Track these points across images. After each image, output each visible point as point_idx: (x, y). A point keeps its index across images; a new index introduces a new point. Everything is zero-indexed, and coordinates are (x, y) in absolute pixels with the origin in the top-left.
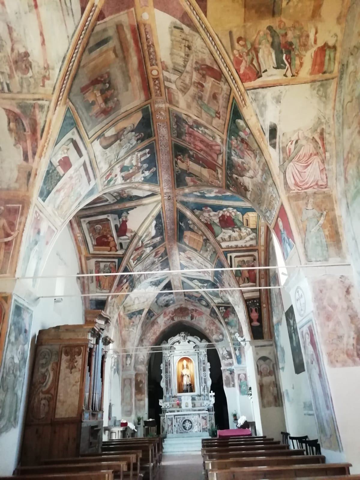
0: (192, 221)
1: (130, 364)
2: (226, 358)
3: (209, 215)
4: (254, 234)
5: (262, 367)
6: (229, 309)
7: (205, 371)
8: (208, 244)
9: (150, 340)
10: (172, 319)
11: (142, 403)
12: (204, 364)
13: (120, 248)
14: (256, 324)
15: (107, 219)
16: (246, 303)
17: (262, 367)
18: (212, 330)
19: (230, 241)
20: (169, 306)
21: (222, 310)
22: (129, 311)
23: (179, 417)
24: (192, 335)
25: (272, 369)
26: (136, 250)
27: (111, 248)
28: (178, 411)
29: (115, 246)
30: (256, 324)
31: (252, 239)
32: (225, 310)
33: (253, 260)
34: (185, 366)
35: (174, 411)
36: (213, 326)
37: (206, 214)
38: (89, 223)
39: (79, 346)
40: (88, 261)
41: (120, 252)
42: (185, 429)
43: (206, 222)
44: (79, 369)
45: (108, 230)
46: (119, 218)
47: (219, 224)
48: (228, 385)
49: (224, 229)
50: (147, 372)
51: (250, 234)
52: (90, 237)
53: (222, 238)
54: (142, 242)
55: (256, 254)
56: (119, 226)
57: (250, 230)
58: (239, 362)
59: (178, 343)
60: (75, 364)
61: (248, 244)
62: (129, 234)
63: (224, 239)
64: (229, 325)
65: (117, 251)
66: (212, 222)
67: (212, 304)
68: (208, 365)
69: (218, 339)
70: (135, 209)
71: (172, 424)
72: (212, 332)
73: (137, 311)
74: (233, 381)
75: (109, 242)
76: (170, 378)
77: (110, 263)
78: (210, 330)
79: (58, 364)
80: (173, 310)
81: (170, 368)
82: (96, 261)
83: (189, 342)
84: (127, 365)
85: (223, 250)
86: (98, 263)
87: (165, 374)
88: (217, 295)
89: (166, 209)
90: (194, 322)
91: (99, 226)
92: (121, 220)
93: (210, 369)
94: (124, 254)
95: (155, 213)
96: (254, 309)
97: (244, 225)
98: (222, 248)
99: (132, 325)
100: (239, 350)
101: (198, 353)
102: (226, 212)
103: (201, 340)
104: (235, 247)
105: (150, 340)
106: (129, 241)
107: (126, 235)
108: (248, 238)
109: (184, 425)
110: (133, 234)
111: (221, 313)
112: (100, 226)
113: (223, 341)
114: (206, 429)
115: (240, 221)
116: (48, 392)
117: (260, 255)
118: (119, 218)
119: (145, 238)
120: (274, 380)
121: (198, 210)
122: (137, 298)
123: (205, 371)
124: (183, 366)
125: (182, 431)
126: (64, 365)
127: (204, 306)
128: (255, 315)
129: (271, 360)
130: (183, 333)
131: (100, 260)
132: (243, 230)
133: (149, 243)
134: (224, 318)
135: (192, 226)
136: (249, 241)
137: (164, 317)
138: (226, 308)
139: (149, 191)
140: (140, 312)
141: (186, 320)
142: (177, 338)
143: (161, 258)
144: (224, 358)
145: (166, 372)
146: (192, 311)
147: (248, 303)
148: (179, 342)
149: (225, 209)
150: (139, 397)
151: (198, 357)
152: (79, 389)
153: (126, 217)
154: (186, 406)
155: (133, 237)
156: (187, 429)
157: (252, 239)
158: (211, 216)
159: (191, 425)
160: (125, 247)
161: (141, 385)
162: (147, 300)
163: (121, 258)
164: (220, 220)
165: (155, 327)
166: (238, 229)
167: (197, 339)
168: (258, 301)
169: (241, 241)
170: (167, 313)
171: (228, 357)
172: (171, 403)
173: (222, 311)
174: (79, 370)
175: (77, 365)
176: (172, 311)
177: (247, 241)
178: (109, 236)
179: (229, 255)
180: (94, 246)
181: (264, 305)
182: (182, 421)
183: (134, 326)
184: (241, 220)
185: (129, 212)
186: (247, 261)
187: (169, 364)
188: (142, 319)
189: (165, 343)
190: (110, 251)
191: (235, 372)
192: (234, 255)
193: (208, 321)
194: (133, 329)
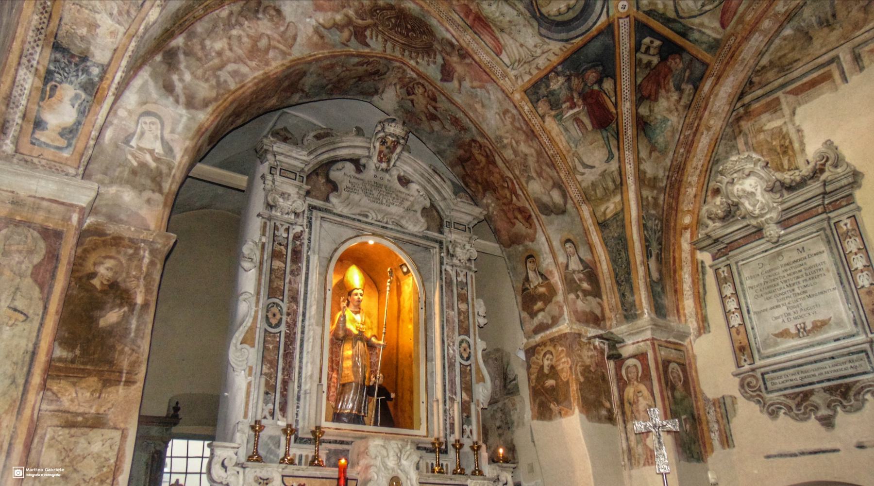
6: (676, 64)
7: (467, 333)
9: (223, 75)
10: (359, 34)
12: (463, 298)
21: (648, 48)
32: (655, 60)
59: (350, 167)
69: (545, 199)
72: (525, 167)
76: (291, 326)
78: (515, 152)
81: (295, 273)
84: (39, 124)
100: (659, 260)
101: (441, 243)
111: (638, 63)
113: (566, 218)
138: (669, 49)
146: (448, 49)
151: (442, 263)
161: (111, 317)
171: (585, 285)
172: (291, 469)
187: (297, 255)
193: (508, 121)
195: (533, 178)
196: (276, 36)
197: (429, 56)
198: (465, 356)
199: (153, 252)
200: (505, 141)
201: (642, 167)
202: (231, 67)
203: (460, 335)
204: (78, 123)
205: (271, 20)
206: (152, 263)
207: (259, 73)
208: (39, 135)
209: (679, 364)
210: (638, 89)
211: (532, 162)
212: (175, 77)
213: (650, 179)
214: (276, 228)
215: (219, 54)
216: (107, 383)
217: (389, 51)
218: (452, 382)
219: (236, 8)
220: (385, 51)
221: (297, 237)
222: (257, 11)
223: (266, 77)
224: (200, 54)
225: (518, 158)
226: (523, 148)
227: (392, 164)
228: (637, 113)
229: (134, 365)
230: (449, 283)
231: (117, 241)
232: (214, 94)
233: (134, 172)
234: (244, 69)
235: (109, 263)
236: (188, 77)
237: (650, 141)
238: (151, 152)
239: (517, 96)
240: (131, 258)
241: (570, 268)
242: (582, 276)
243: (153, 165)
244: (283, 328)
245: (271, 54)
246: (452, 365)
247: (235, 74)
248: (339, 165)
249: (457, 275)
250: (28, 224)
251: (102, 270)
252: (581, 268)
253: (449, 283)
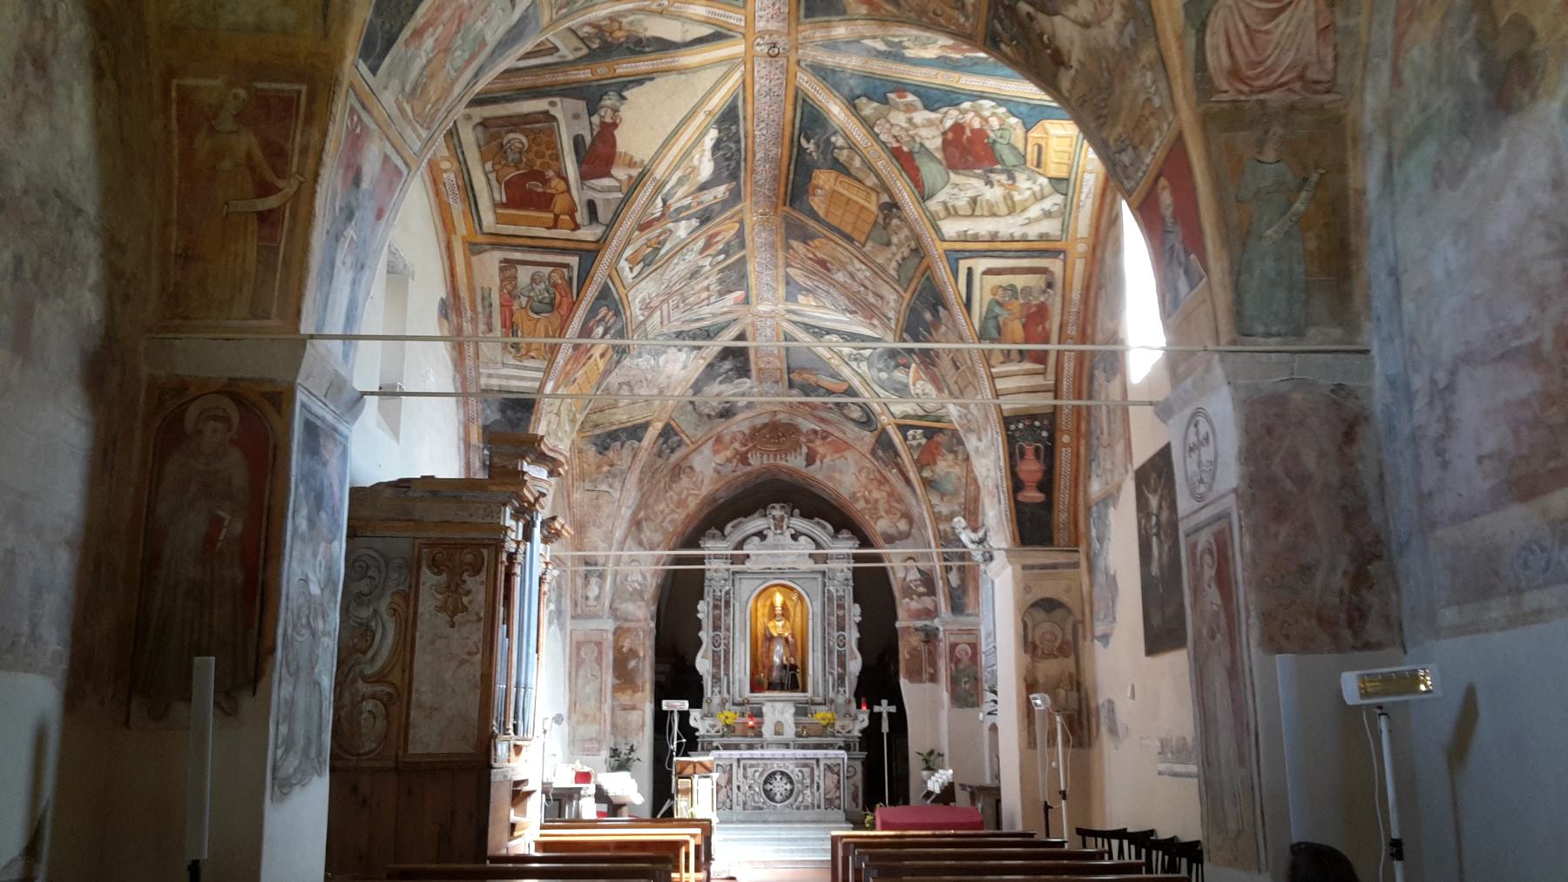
0: (846, 137)
1: (598, 598)
2: (915, 592)
3: (910, 120)
4: (1058, 199)
5: (1038, 632)
6: (939, 438)
7: (843, 630)
8: (895, 222)
9: (665, 524)
11: (634, 716)
12: (841, 607)
13: (586, 222)
14: (1032, 495)
15: (546, 113)
16: (1007, 429)
17: (1038, 632)
18: (877, 501)
19: (972, 215)
20: (735, 414)
21: (914, 438)
22: (596, 426)
23: (754, 762)
24: (807, 515)
25: (1069, 637)
26: (643, 227)
27: (557, 217)
28: (751, 747)
29: (572, 212)
30: (1032, 495)
31: (1048, 214)
32: (924, 441)
33: (1043, 285)
34: (779, 610)
35: (736, 747)
36: (879, 489)
37: (899, 118)
38: (484, 124)
39: (477, 545)
40: (474, 259)
41: (588, 234)
42: (772, 799)
43: (896, 145)
44: (477, 614)
45: (548, 153)
46: (590, 115)
47: (939, 155)
48: (915, 676)
49: (957, 173)
50: (653, 625)
51: (1043, 198)
52: (486, 174)
53: (945, 204)
54: (664, 201)
55: (1055, 266)
56: (588, 140)
57: (1044, 181)
58: (957, 607)
59: (756, 539)
60: (465, 600)
61: (1033, 232)
62: (620, 173)
63: (954, 207)
64: (932, 487)
65: (577, 227)
66: (917, 146)
67: (884, 419)
68: (854, 612)
69: (892, 531)
70: (648, 84)
71: (730, 781)
73: (624, 429)
74: (933, 663)
75: (553, 196)
76: (727, 645)
77: (551, 269)
78: (867, 501)
79: (410, 597)
80: (747, 431)
82: (506, 261)
83: (794, 537)
84: (587, 598)
85: (947, 246)
86: (508, 264)
87: (711, 634)
88: (902, 391)
89: (757, 87)
90: (817, 473)
91: (518, 139)
92: (596, 119)
93: (859, 625)
94: (602, 242)
95: (718, 101)
96: (1029, 449)
97: (1028, 164)
98: (943, 240)
99: (609, 472)
102: (971, 115)
103: (837, 530)
104: (988, 238)
105: (665, 524)
106: (621, 196)
107: (612, 176)
108: (1035, 211)
109: (769, 787)
110: (635, 172)
111: (910, 447)
112: (524, 140)
114: (837, 802)
115: (1014, 148)
116: (380, 678)
117: (1068, 268)
118: (590, 115)
119: (673, 188)
120: (1073, 669)
121: (870, 99)
122: (628, 384)
123: (843, 630)
124: (773, 606)
125: (760, 804)
126: (428, 602)
127: (853, 420)
128: (1031, 468)
129: (1069, 611)
130: (778, 506)
131: (517, 256)
132: (1023, 182)
133: (688, 207)
134: (921, 465)
135: (843, 156)
136: (1037, 220)
137: (716, 452)
138: (930, 433)
139: (706, 22)
140: (636, 432)
141: (790, 464)
142: (756, 523)
143: (722, 257)
144: (908, 592)
145: (716, 628)
146: (812, 437)
147: (1013, 427)
148: (761, 535)
149: (966, 105)
150: (625, 698)
151: (824, 585)
152: (478, 676)
153: (615, 111)
154: (777, 733)
155: (636, 184)
156: (778, 797)
157: (1048, 214)
158: (916, 127)
159: (788, 787)
160: (604, 214)
161: (632, 664)
162: (661, 392)
163: (589, 255)
164: (945, 142)
165: (685, 481)
166: (1003, 178)
167: (824, 528)
168: (1046, 422)
169: (1010, 220)
170: (727, 438)
171: (922, 589)
173: (914, 443)
174: (479, 620)
175: (471, 602)
176: (744, 434)
177: (1030, 222)
178: (550, 173)
179: (964, 265)
180: (497, 205)
181: (1066, 439)
182: (761, 775)
183: (615, 476)
184: (1020, 146)
185: (625, 94)
186: (1023, 289)
187: (727, 603)
188: (643, 456)
189: (714, 537)
190: (555, 226)
191: (941, 635)
192: (981, 265)
193: (864, 475)
194: (611, 486)
195: (882, 517)
196: (692, 486)
197: (796, 451)
198: (841, 644)
199: (644, 631)
200: (859, 495)
201: (936, 510)
202: (668, 518)
203: (838, 631)
204: (600, 593)
205: (688, 477)
206: (644, 637)
207: (683, 516)
208: (590, 603)
209: (968, 644)
210: (916, 462)
211: (882, 506)
212: (642, 536)
213: (946, 516)
214: (714, 591)
215: (662, 512)
216: (635, 691)
217: (765, 462)
218: (831, 662)
219: (667, 479)
220: (762, 463)
221: (727, 593)
222: (679, 474)
223: (688, 515)
224: (652, 517)
225: (870, 506)
226: (876, 494)
227: (785, 527)
228: (921, 477)
229: (644, 683)
230: (830, 599)
231: (628, 630)
232: (662, 538)
233: (632, 595)
234: (675, 516)
235: (628, 640)
236: (648, 533)
237: (938, 491)
238: (637, 581)
239: (869, 456)
240: (636, 636)
241: (908, 579)
242: (919, 583)
243: (638, 587)
244: (722, 647)
245: (690, 499)
246: (831, 652)
247: (671, 521)
248: (748, 541)
249: (837, 591)
250: (590, 642)
251: (626, 644)
252: (919, 576)
253: (830, 599)
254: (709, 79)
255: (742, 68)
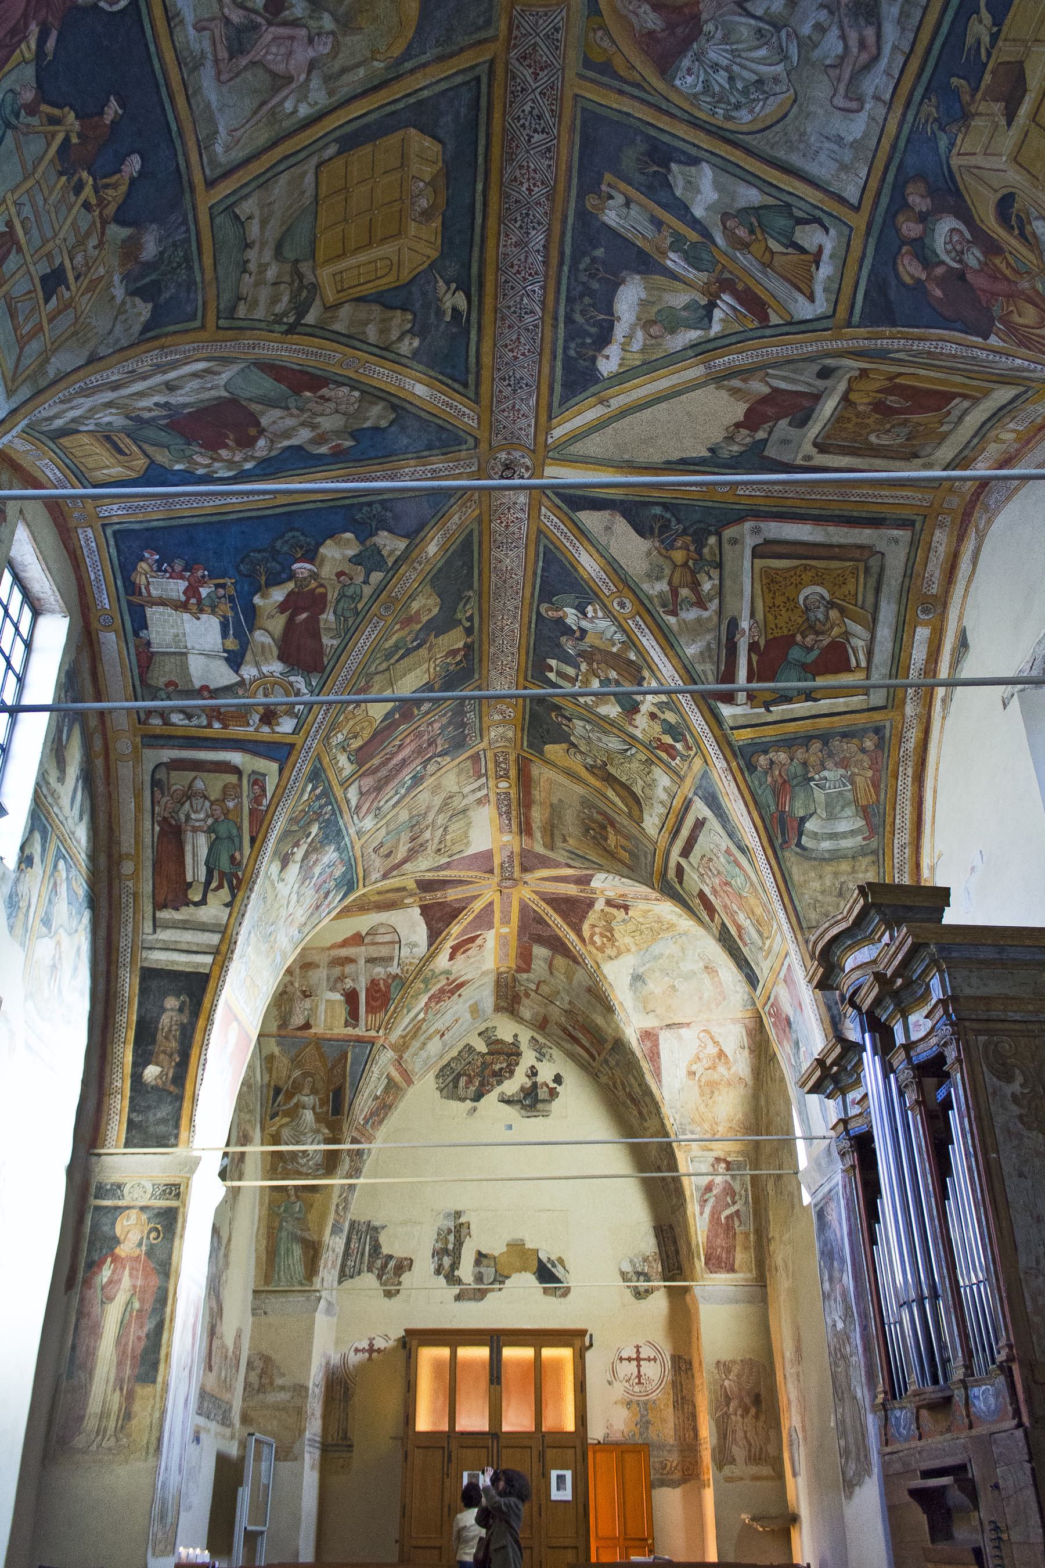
3: (314, 427)
43: (324, 391)
47: (255, 407)
70: (676, 456)
89: (532, 402)
92: (761, 435)
121: (376, 429)
133: (677, 243)
139: (582, 533)
153: (730, 439)
158: (303, 424)
254: (592, 446)
255: (550, 441)
